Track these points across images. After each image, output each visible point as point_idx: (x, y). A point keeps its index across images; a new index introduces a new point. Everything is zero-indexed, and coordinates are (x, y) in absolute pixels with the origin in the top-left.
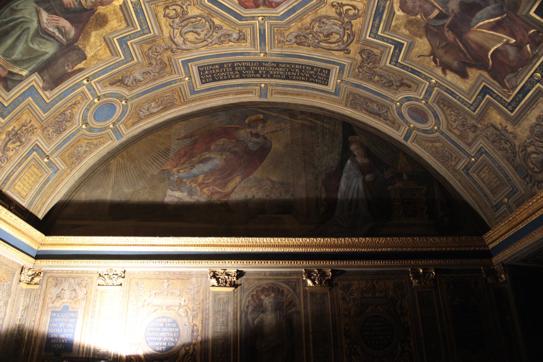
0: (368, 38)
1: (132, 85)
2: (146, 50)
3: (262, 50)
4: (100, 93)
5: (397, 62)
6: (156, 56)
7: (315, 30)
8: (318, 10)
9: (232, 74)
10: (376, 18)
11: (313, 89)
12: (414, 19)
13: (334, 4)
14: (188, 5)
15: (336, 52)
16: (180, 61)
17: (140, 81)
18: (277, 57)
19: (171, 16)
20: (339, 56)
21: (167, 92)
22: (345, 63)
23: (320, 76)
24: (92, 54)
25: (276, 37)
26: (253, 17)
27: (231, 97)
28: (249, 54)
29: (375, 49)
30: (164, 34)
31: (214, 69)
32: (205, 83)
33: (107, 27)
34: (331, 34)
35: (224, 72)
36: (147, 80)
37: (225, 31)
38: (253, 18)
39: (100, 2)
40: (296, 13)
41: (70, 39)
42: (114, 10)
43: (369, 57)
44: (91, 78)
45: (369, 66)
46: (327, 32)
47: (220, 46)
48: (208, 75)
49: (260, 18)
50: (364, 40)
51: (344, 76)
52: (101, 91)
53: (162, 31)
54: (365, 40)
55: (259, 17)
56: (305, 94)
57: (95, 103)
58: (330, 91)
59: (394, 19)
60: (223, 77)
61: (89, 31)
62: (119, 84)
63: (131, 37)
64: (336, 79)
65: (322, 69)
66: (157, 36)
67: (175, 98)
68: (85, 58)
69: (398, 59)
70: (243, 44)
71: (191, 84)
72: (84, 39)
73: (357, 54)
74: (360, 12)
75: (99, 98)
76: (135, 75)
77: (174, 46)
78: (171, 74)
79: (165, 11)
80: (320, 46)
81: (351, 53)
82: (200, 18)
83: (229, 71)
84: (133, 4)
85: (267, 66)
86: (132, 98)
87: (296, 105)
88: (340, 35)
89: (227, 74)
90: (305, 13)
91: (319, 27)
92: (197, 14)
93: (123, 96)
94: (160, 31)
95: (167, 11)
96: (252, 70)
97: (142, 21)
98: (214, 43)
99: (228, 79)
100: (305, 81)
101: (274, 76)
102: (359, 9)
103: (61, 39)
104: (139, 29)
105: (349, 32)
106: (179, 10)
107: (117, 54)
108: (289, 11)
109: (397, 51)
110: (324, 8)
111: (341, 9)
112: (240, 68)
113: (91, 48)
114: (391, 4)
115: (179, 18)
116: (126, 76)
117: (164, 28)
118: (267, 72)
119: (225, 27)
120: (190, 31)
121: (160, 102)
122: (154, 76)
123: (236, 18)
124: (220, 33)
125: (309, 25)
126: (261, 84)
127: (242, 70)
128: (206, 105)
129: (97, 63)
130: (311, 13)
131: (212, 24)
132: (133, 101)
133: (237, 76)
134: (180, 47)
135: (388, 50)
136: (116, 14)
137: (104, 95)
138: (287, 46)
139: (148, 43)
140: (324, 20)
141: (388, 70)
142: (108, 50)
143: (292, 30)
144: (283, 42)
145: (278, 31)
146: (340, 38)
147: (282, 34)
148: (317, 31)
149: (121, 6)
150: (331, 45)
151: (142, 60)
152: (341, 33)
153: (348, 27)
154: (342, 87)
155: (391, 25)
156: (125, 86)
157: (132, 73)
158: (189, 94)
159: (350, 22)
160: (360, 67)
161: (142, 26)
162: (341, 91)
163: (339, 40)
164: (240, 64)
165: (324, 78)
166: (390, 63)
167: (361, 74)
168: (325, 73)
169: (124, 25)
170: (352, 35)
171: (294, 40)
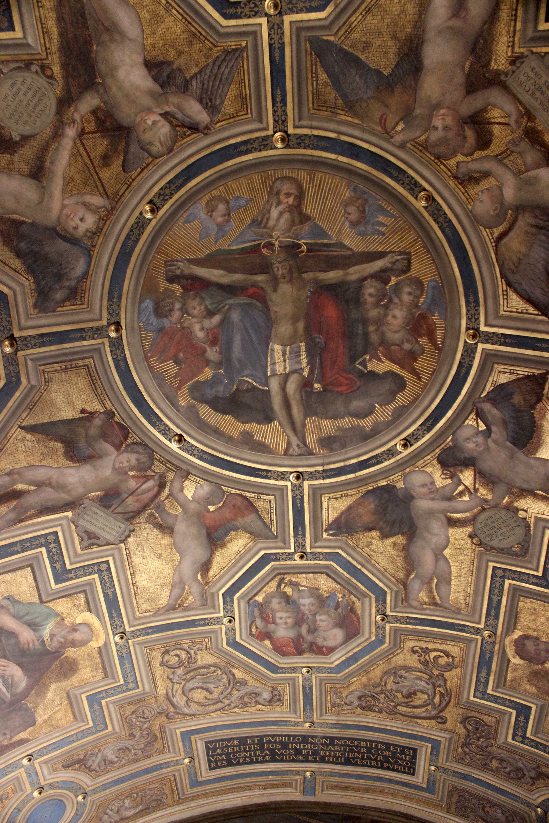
0: (472, 698)
1: (98, 769)
2: (128, 713)
3: (307, 718)
4: (45, 780)
5: (524, 737)
6: (142, 724)
7: (388, 688)
8: (392, 658)
9: (259, 755)
11: (390, 781)
12: (541, 670)
13: (416, 648)
14: (199, 649)
15: (423, 721)
16: (178, 731)
17: (112, 762)
18: (330, 728)
19: (171, 665)
20: (430, 728)
21: (152, 781)
22: (439, 739)
23: (401, 759)
24: (45, 717)
25: (329, 698)
26: (294, 668)
27: (257, 792)
28: (285, 723)
29: (485, 717)
30: (158, 690)
31: (230, 746)
32: (214, 768)
33: (74, 677)
34: (415, 693)
35: (246, 752)
36: (124, 762)
37: (251, 688)
38: (294, 669)
39: (71, 643)
40: (359, 663)
41: (17, 694)
42: (89, 654)
43: (477, 729)
44: (35, 756)
45: (480, 743)
46: (408, 691)
47: (242, 710)
48: (221, 755)
49: (304, 670)
50: (466, 702)
51: (440, 760)
52: (48, 777)
53: (156, 686)
54: (468, 701)
55: (302, 667)
56: (377, 789)
57: (34, 798)
58: (419, 784)
59: (510, 669)
60: (245, 760)
61: (47, 683)
62: (77, 766)
63: (108, 693)
64: (427, 765)
65: (403, 748)
66: (148, 693)
67: (164, 793)
68: (33, 723)
69: (525, 731)
70: (278, 708)
71: (192, 770)
72: (38, 694)
73: (458, 725)
74: (456, 660)
75: (41, 790)
76: (105, 752)
77: (172, 709)
78: (162, 752)
79: (163, 658)
80: (397, 711)
81: (449, 722)
82: (214, 669)
83: (255, 750)
84: (118, 646)
85: (317, 744)
86: (95, 791)
87: (363, 808)
88: (428, 695)
89: (251, 754)
90: (372, 662)
91: (395, 683)
92: (210, 663)
93: (81, 788)
94: (153, 685)
95: (167, 657)
96: (292, 749)
97: (128, 671)
98: (233, 705)
99: (252, 762)
100: (376, 767)
101: (327, 759)
103: (3, 693)
104: (122, 682)
105: (441, 690)
106: (184, 657)
107: (84, 719)
108: (348, 659)
109: (522, 719)
110: (401, 656)
111: (427, 657)
112: (273, 746)
113: (45, 708)
114: (501, 648)
115: (182, 668)
116: (92, 754)
117: (159, 682)
118: (315, 753)
119: (251, 682)
120: (197, 688)
121: (139, 799)
122: (135, 754)
123: (268, 669)
124: (244, 690)
125: (379, 680)
126: (305, 771)
127: (275, 748)
128: (215, 806)
129: (51, 731)
130: (381, 663)
131: (231, 677)
132: (96, 797)
133: (267, 758)
134: (181, 710)
135: (507, 717)
136: (91, 660)
137: (51, 784)
138: (346, 712)
139: (132, 703)
140: (402, 672)
141: (511, 750)
142: (70, 712)
143: (353, 687)
144: (339, 705)
145: (332, 689)
146: (429, 699)
147: (337, 693)
148: (392, 689)
149: (100, 648)
150: (415, 710)
151: (120, 729)
152: (430, 693)
153: (439, 682)
154: (438, 777)
155: (506, 679)
156: (87, 771)
157: (102, 749)
158: (188, 786)
159: (443, 676)
160: (464, 745)
161: (127, 678)
162: (437, 785)
163: (428, 702)
164: (273, 738)
165: (407, 764)
166: (513, 739)
167: (467, 757)
168: (409, 755)
169: (101, 675)
170: (446, 695)
171: (357, 703)
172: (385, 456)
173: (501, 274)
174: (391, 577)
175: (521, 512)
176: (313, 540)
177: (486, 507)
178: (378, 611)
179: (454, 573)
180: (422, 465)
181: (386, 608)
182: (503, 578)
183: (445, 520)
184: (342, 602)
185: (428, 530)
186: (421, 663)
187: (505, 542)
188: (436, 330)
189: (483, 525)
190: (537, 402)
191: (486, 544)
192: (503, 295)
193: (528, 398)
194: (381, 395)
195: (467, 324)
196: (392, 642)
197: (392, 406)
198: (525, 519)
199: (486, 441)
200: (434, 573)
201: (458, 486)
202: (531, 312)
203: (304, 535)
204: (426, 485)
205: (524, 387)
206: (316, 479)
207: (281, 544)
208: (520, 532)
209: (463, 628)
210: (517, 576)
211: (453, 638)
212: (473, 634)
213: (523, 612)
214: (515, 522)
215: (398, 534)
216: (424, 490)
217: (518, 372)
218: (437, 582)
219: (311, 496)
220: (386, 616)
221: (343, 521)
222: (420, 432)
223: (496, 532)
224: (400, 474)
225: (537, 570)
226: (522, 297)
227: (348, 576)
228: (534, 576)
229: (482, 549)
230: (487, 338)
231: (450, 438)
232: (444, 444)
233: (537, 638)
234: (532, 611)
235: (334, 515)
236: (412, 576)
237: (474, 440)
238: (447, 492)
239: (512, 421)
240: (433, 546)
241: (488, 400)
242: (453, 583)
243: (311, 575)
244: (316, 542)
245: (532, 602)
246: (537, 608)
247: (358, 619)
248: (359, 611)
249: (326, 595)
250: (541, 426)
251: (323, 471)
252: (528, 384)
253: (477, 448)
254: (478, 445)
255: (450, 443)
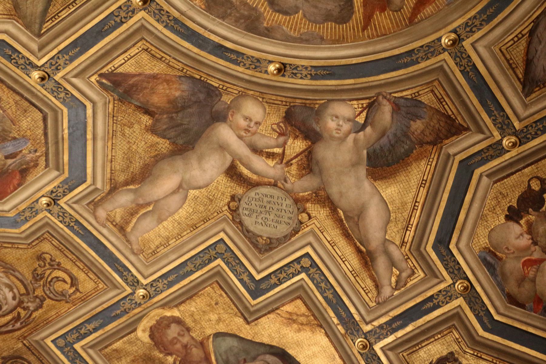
0: (48, 341)
8: (6, 247)
10: (96, 320)
12: (159, 359)
13: (47, 256)
50: (37, 342)
102: (81, 289)
105: (23, 313)
111: (48, 272)
153: (30, 304)
155: (110, 345)
159: (42, 301)
172: (248, 63)
173: (537, 18)
174: (109, 171)
175: (305, 215)
176: (75, 72)
177: (279, 184)
178: (52, 192)
179: (176, 217)
180: (268, 101)
181: (64, 195)
182: (219, 255)
183: (228, 164)
184: (24, 156)
185: (200, 159)
186: (33, 273)
187: (260, 227)
188: (430, 4)
189: (257, 197)
190: (427, 143)
191: (239, 215)
192: (516, 36)
193: (427, 132)
194: (316, 7)
195: (460, 26)
196: (28, 232)
197: (314, 28)
198: (301, 223)
199: (349, 133)
200: (157, 201)
201: (278, 146)
202: (518, 72)
203: (72, 60)
204: (251, 120)
205: (435, 121)
206: (158, 21)
207: (34, 46)
208: (283, 230)
209: (122, 270)
210: (234, 263)
211: (100, 274)
212: (127, 284)
213: (203, 297)
214: (290, 218)
215: (168, 139)
216: (243, 123)
217: (446, 106)
218: (149, 211)
219: (131, 30)
220: (55, 202)
221: (131, 82)
222: (304, 72)
223: (261, 212)
224: (240, 89)
225: (259, 272)
226: (527, 53)
227: (66, 136)
228: (250, 275)
229: (231, 217)
230: (459, 54)
231: (323, 101)
232: (311, 102)
233: (188, 330)
234: (213, 303)
235: (129, 68)
236: (132, 187)
237: (341, 123)
238: (261, 142)
239: (391, 137)
240: (187, 176)
241: (394, 102)
242: (165, 223)
243: (26, 104)
244: (76, 76)
245: (221, 295)
246: (220, 304)
247: (19, 185)
248: (30, 178)
249: (16, 135)
250: (409, 164)
251: (176, 20)
252: (441, 122)
253: (334, 132)
254: (340, 130)
255: (317, 106)
